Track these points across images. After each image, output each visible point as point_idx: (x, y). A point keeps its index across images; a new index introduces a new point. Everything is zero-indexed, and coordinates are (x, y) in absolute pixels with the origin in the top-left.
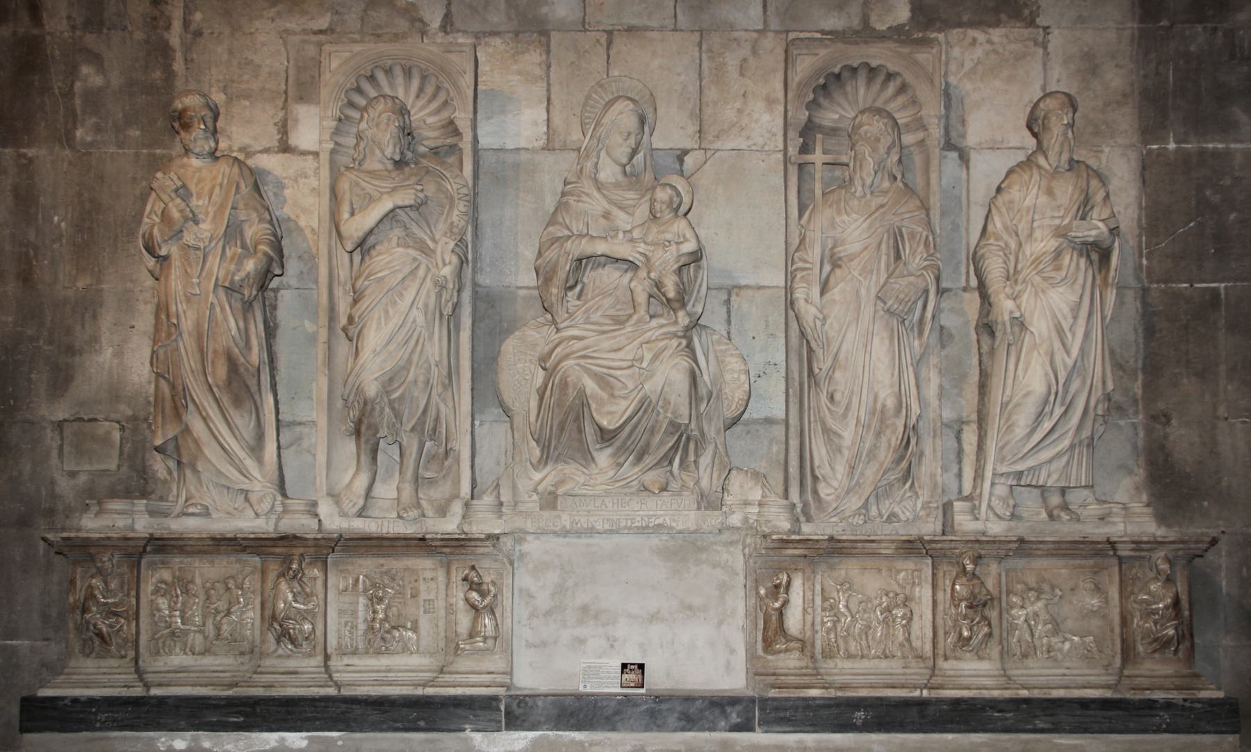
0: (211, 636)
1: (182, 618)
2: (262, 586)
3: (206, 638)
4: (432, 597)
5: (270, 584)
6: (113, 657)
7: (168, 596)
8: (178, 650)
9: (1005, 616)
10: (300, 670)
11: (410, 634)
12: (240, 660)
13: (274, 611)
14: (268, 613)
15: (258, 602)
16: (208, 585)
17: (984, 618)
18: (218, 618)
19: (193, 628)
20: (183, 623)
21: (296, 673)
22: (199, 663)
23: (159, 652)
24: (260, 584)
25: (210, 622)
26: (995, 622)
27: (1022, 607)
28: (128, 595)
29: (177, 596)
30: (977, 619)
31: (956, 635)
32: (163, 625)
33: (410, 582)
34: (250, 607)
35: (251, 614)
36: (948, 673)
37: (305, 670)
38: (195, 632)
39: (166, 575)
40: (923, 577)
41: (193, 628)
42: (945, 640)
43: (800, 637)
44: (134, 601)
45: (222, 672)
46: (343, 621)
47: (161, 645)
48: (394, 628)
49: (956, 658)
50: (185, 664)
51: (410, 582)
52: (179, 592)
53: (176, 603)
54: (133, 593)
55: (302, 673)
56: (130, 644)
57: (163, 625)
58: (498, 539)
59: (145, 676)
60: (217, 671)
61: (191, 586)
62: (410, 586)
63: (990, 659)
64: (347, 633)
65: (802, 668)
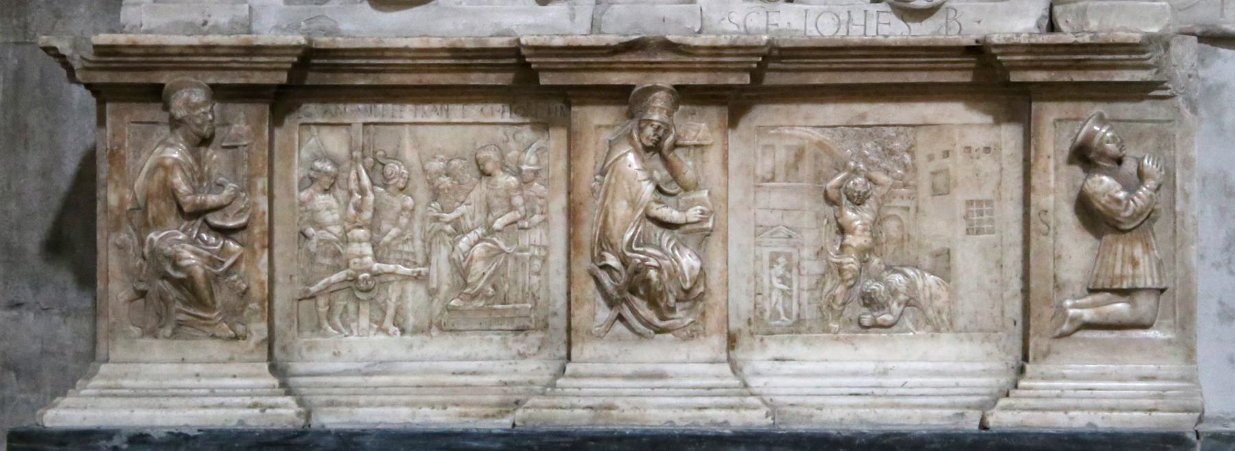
0: (445, 288)
2: (569, 167)
3: (432, 293)
4: (987, 194)
5: (588, 165)
7: (341, 194)
8: (364, 322)
10: (668, 368)
11: (931, 279)
13: (605, 227)
14: (588, 232)
15: (558, 204)
18: (463, 244)
19: (402, 269)
20: (377, 259)
21: (661, 376)
22: (416, 352)
23: (319, 326)
24: (562, 165)
25: (441, 257)
28: (249, 188)
32: (327, 261)
33: (931, 158)
34: (537, 218)
35: (536, 236)
38: (406, 278)
39: (334, 142)
41: (402, 269)
44: (264, 205)
45: (474, 373)
46: (766, 253)
47: (323, 310)
48: (889, 268)
50: (384, 354)
51: (931, 158)
52: (366, 181)
53: (359, 209)
54: (262, 183)
55: (677, 376)
56: (254, 305)
57: (327, 261)
58: (1167, 46)
59: (292, 381)
60: (462, 373)
61: (393, 167)
62: (932, 167)
64: (777, 284)
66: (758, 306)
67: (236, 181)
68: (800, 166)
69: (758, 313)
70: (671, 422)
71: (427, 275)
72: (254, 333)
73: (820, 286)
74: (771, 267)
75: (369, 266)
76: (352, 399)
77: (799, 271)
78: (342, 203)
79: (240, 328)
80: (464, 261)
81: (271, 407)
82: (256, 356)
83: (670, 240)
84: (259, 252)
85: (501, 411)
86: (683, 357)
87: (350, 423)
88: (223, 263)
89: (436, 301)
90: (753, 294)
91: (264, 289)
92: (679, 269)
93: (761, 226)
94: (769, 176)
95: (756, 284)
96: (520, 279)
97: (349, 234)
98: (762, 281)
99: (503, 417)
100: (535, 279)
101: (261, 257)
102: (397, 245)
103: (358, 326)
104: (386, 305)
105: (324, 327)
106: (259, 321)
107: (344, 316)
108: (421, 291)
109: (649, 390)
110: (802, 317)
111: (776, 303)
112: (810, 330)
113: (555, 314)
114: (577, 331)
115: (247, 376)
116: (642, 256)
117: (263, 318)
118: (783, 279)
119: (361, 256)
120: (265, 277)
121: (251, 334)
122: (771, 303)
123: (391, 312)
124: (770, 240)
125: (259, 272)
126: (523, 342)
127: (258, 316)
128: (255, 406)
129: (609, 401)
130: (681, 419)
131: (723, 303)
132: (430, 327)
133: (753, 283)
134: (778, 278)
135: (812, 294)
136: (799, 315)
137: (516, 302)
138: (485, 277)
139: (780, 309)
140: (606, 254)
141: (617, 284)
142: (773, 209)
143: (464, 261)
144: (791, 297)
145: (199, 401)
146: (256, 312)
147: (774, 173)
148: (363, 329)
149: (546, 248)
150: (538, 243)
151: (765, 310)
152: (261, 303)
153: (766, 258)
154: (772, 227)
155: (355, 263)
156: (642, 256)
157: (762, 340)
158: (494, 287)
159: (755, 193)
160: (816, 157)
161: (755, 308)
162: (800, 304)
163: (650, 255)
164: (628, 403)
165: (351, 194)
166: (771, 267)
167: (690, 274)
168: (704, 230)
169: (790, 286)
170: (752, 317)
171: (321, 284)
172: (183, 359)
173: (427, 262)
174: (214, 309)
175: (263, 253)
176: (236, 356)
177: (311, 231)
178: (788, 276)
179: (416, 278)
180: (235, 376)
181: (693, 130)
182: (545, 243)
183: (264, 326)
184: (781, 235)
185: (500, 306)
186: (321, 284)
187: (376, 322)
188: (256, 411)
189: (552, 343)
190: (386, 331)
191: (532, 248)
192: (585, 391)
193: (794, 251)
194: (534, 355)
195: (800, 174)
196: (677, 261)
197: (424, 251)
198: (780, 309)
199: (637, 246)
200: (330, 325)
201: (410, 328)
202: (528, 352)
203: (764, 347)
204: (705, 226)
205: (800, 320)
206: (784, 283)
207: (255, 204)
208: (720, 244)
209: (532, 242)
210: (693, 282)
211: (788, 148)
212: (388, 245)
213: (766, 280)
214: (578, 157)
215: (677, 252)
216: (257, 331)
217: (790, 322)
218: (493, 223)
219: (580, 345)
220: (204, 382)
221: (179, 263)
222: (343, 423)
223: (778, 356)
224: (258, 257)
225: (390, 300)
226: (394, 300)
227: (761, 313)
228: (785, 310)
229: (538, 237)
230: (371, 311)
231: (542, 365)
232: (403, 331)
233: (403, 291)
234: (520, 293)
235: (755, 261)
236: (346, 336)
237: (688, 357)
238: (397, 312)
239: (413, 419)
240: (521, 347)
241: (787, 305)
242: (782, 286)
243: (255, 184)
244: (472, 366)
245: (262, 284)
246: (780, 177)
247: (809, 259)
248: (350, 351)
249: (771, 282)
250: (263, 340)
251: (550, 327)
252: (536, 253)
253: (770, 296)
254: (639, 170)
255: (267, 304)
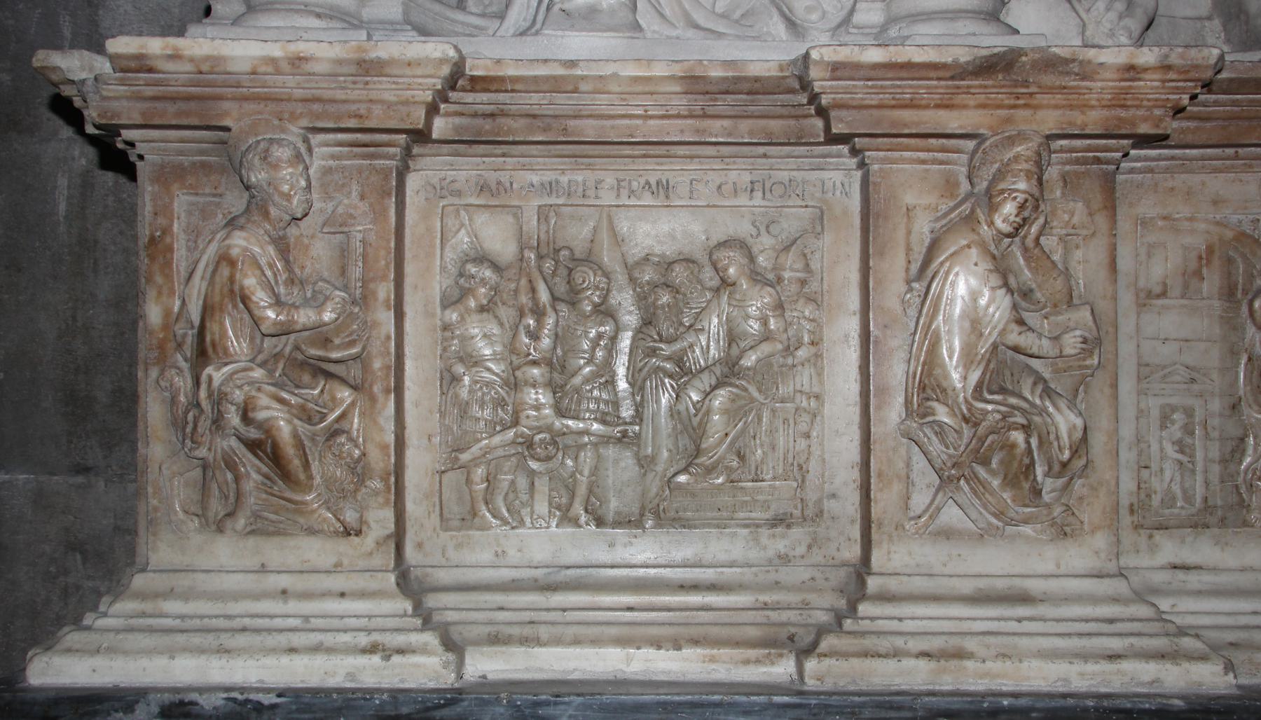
1: (555, 388)
3: (646, 463)
6: (311, 531)
10: (1035, 586)
12: (777, 543)
16: (647, 275)
20: (561, 412)
21: (1024, 598)
23: (474, 513)
28: (365, 300)
29: (539, 314)
37: (1053, 585)
45: (713, 587)
46: (1154, 405)
52: (544, 296)
53: (535, 336)
56: (376, 484)
59: (432, 601)
66: (1142, 485)
67: (345, 288)
68: (1205, 271)
69: (1143, 496)
70: (1065, 680)
71: (638, 436)
72: (373, 524)
73: (1237, 456)
74: (1163, 427)
75: (549, 421)
76: (527, 631)
77: (1207, 433)
78: (507, 326)
79: (350, 516)
80: (696, 415)
81: (401, 651)
82: (377, 561)
83: (1035, 384)
84: (381, 398)
85: (769, 654)
86: (1050, 567)
87: (527, 669)
88: (323, 417)
89: (650, 476)
90: (1136, 467)
91: (389, 457)
92: (1052, 429)
93: (1147, 365)
94: (1158, 289)
95: (1140, 454)
96: (781, 442)
97: (518, 373)
98: (1149, 446)
99: (773, 664)
100: (802, 444)
101: (385, 406)
102: (591, 391)
103: (532, 512)
104: (575, 481)
105: (481, 513)
106: (382, 506)
107: (511, 496)
108: (627, 458)
109: (1014, 624)
110: (1210, 503)
111: (1171, 481)
112: (1223, 522)
113: (834, 496)
114: (880, 525)
115: (363, 595)
116: (1002, 408)
117: (387, 502)
118: (1181, 447)
119: (537, 407)
120: (391, 439)
121: (369, 527)
122: (1162, 481)
123: (582, 491)
124: (1163, 386)
125: (382, 430)
126: (783, 536)
127: (381, 500)
128: (372, 649)
129: (954, 642)
130: (1082, 674)
131: (1113, 483)
132: (642, 515)
133: (1134, 453)
134: (1173, 443)
135: (1226, 468)
136: (1206, 500)
137: (774, 478)
138: (729, 439)
139: (1176, 488)
140: (935, 404)
141: (951, 451)
142: (1166, 339)
143: (696, 415)
144: (1193, 472)
145: (282, 640)
146: (376, 493)
147: (1165, 284)
148: (539, 517)
149: (817, 397)
150: (806, 388)
151: (1155, 493)
152: (385, 479)
153: (1155, 413)
154: (1164, 367)
155: (528, 417)
156: (1002, 408)
157: (1151, 537)
158: (741, 457)
159: (1138, 314)
160: (1230, 261)
161: (1139, 488)
162: (1207, 483)
163: (1013, 407)
164: (988, 647)
165: (522, 315)
166: (1163, 427)
167: (1070, 437)
168: (1087, 367)
169: (1192, 456)
170: (1135, 501)
171: (475, 450)
172: (263, 565)
173: (638, 417)
174: (309, 488)
175: (387, 399)
176: (346, 562)
177: (459, 369)
178: (1189, 440)
179: (619, 440)
180: (342, 595)
181: (1064, 212)
182: (816, 389)
183: (389, 514)
184: (1178, 378)
185: (750, 484)
186: (475, 450)
187: (559, 508)
188: (376, 659)
189: (829, 539)
190: (575, 522)
191: (798, 395)
192: (909, 626)
193: (1197, 404)
194: (803, 557)
195: (1205, 286)
196: (1049, 415)
197: (634, 400)
198: (1176, 488)
199: (991, 393)
200: (489, 511)
201: (610, 517)
202: (791, 554)
203: (1153, 549)
204: (1088, 362)
205: (1207, 507)
206: (1182, 451)
207: (375, 324)
208: (1107, 390)
209: (798, 387)
210: (1074, 449)
211: (1185, 248)
212: (577, 390)
213: (1155, 447)
214: (881, 254)
215: (1048, 403)
216: (377, 522)
217: (1194, 511)
218: (740, 358)
219: (885, 546)
220: (293, 606)
221: (251, 415)
222: (516, 671)
223: (1178, 561)
224: (379, 406)
225: (581, 474)
226: (586, 473)
227: (1149, 496)
228: (1184, 491)
229: (806, 380)
230: (551, 490)
231: (818, 575)
232: (600, 522)
233: (599, 457)
234: (781, 464)
235: (1137, 419)
236: (513, 528)
237: (1058, 566)
238: (591, 491)
239: (628, 665)
240: (781, 546)
241: (1187, 485)
242: (1180, 456)
243: (374, 293)
244: (708, 574)
245: (385, 447)
246: (1177, 291)
247: (1221, 415)
248: (519, 551)
249: (1162, 450)
250: (389, 537)
251: (826, 515)
252: (805, 404)
253: (1162, 470)
254: (990, 271)
255: (393, 479)
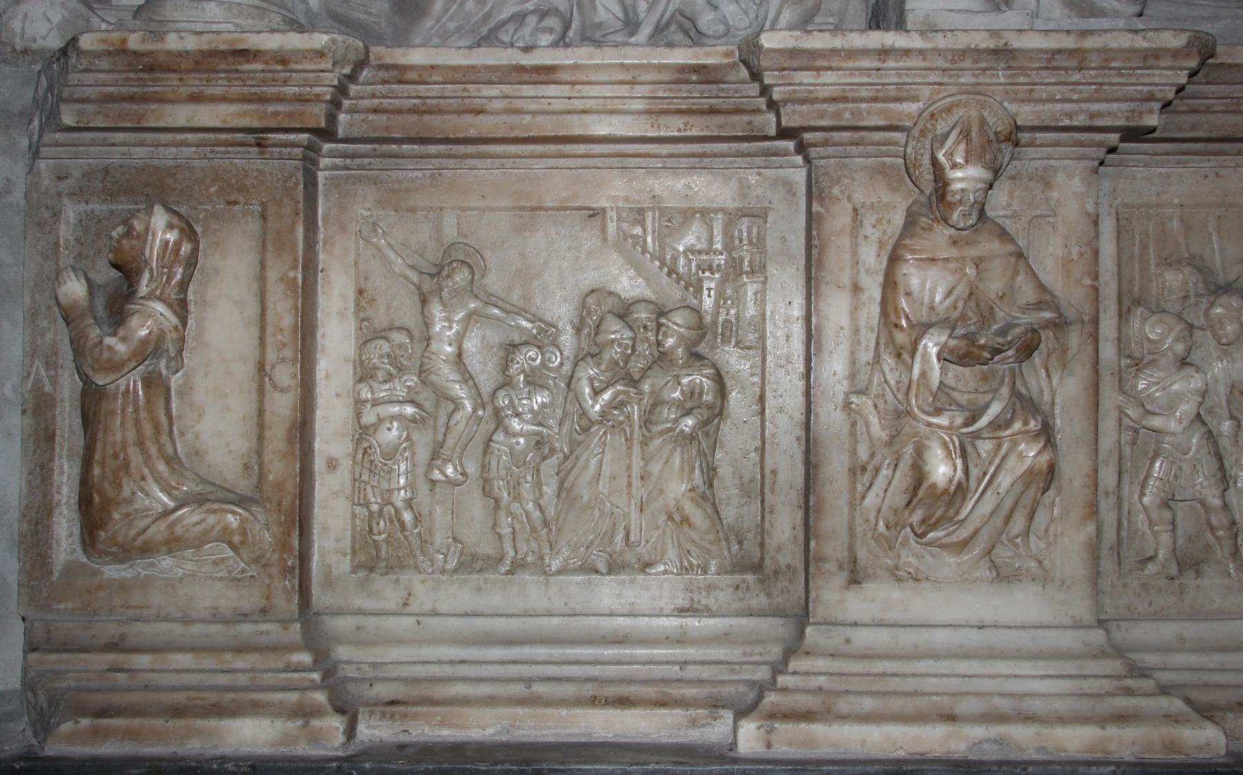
9: (1110, 398)
17: (1025, 404)
26: (1068, 425)
27: (1183, 362)
30: (995, 409)
31: (902, 479)
36: (864, 638)
40: (771, 243)
42: (855, 502)
43: (244, 486)
49: (896, 575)
63: (1044, 578)
65: (242, 617)
